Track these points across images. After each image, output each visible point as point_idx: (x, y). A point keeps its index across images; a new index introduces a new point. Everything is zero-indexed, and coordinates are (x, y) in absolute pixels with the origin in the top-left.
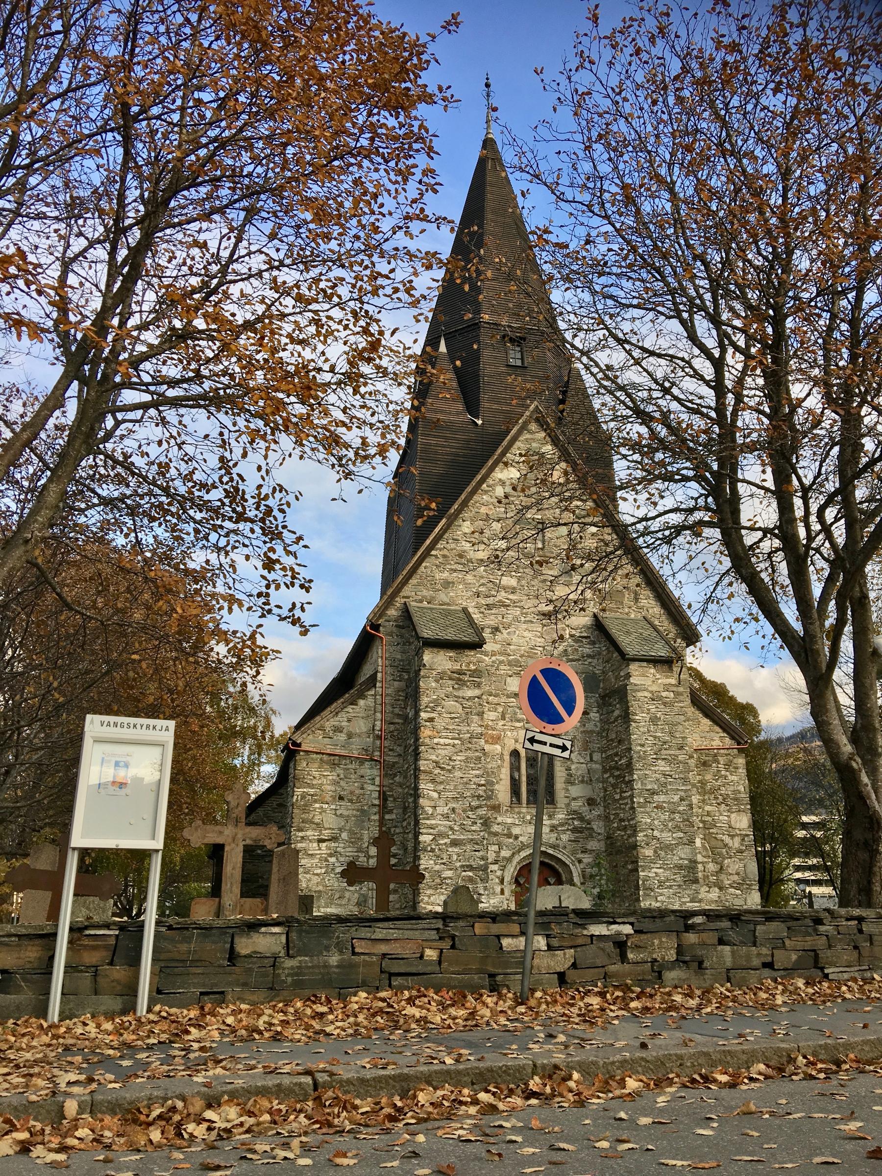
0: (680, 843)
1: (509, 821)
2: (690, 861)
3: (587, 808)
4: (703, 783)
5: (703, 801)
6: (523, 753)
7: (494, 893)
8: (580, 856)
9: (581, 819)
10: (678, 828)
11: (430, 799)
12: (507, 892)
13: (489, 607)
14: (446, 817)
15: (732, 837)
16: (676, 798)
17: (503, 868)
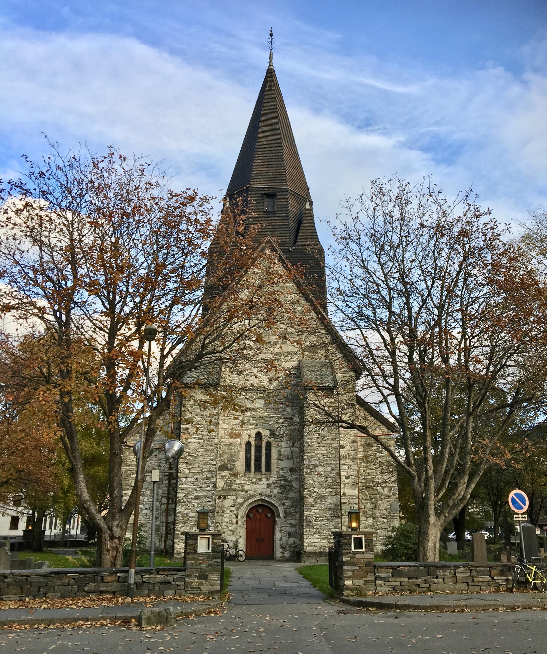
0: (330, 495)
1: (243, 482)
2: (336, 505)
3: (290, 474)
4: (366, 457)
5: (367, 467)
6: (253, 443)
7: (232, 524)
8: (284, 501)
9: (286, 480)
10: (329, 486)
11: (184, 473)
12: (239, 523)
14: (193, 483)
15: (383, 488)
16: (329, 469)
17: (238, 509)
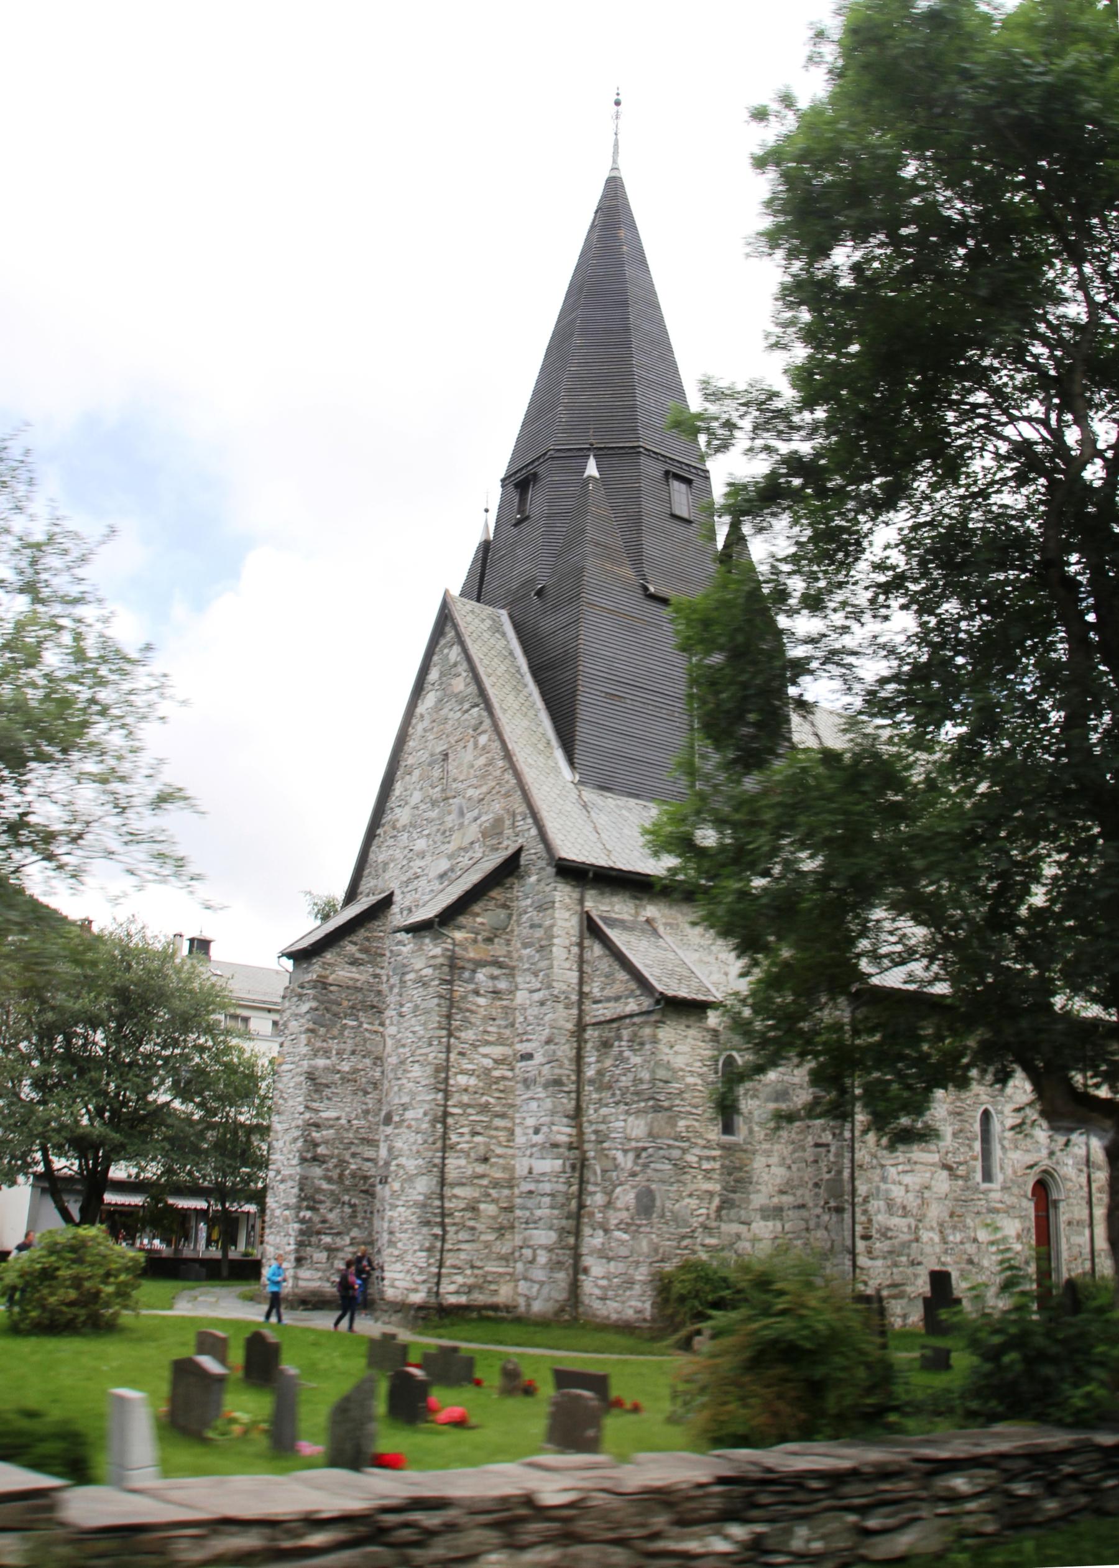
4: (600, 1073)
13: (408, 882)
15: (625, 1151)
